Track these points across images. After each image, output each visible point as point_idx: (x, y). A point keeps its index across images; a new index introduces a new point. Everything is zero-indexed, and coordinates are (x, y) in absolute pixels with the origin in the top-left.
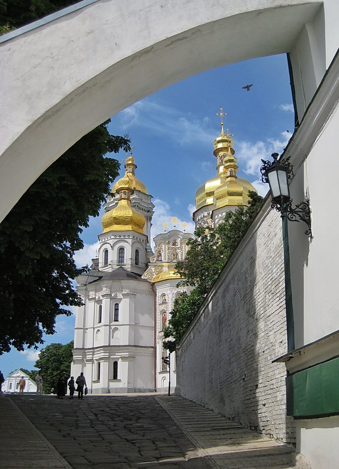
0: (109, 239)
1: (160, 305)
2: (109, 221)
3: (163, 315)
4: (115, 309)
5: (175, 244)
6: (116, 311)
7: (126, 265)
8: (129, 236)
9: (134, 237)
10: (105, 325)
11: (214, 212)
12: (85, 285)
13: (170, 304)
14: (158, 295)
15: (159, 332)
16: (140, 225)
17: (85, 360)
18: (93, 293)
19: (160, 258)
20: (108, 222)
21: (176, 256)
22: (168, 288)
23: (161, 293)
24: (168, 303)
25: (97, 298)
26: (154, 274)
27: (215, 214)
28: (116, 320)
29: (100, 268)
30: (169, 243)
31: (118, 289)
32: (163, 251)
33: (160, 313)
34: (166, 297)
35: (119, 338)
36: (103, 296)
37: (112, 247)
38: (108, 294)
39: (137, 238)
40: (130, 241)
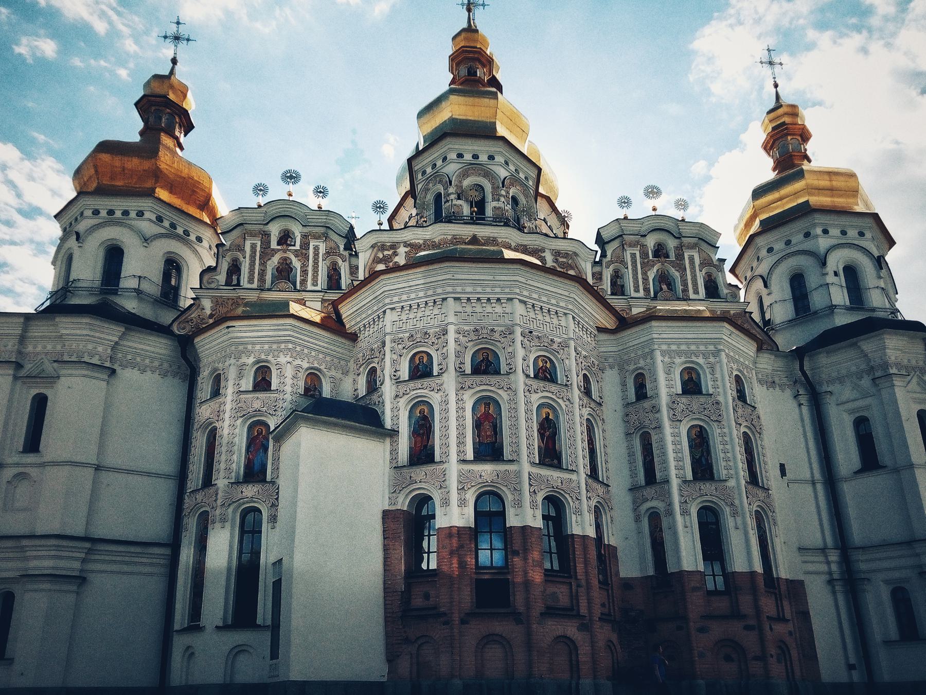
9: (160, 219)
19: (235, 277)
39: (173, 226)
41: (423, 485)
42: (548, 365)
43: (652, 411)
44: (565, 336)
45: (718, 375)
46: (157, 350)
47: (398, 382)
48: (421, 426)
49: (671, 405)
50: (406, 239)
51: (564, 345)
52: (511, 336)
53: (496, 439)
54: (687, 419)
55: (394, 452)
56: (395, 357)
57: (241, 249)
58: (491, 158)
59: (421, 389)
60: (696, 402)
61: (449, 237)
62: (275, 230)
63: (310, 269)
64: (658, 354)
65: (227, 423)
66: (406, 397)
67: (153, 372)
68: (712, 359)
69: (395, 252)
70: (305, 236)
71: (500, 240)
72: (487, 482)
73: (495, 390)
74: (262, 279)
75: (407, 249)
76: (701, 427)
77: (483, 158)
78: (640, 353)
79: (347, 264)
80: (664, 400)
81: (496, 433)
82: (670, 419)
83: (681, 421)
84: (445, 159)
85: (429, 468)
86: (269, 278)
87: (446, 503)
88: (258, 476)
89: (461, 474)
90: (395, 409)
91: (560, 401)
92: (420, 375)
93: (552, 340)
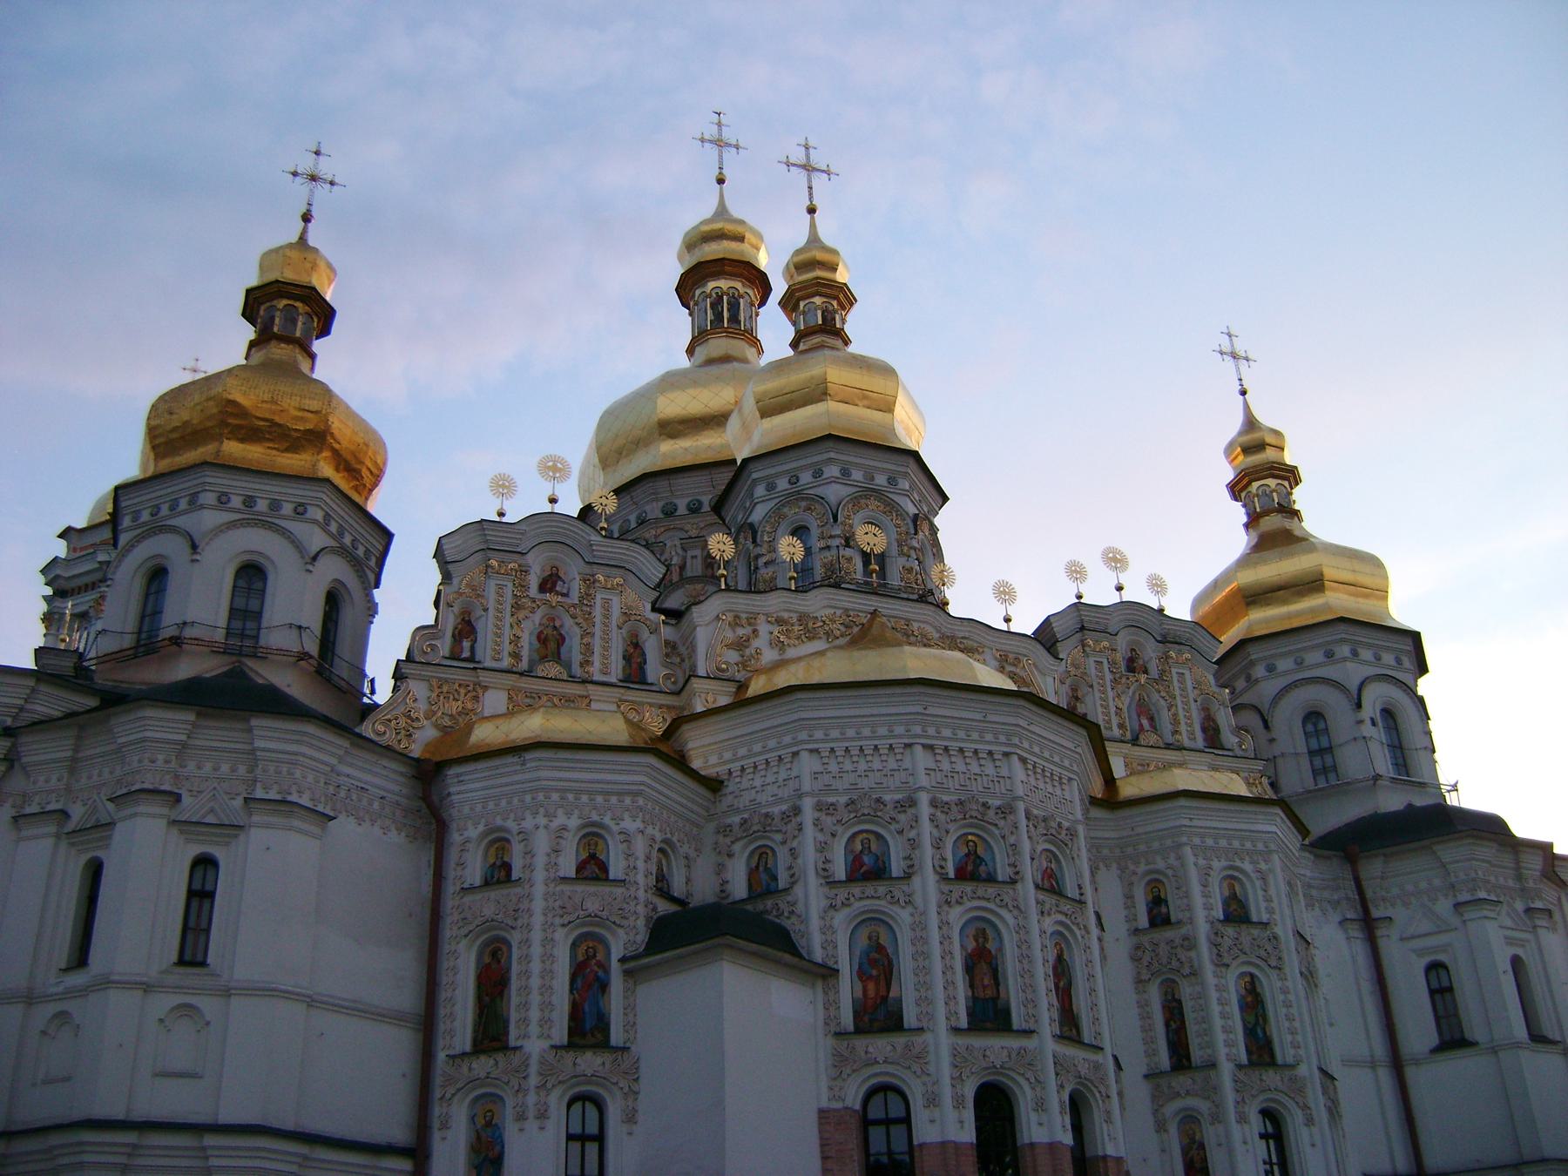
0: (183, 504)
3: (487, 959)
4: (191, 894)
5: (554, 585)
6: (195, 904)
8: (300, 509)
9: (327, 517)
11: (751, 466)
15: (452, 1057)
16: (355, 470)
19: (466, 644)
21: (552, 645)
23: (481, 828)
27: (754, 476)
28: (188, 957)
31: (225, 768)
39: (341, 532)
41: (890, 1069)
42: (1053, 866)
43: (1182, 946)
44: (1070, 817)
45: (1272, 892)
46: (392, 786)
47: (832, 883)
48: (873, 963)
49: (1213, 936)
50: (771, 609)
51: (1072, 833)
52: (1012, 817)
53: (998, 991)
54: (1240, 960)
55: (831, 1005)
56: (820, 837)
57: (477, 592)
58: (892, 481)
59: (868, 899)
60: (1247, 935)
61: (839, 612)
62: (537, 566)
64: (1187, 850)
65: (537, 935)
66: (846, 911)
67: (373, 822)
68: (1263, 866)
69: (755, 631)
70: (589, 581)
71: (916, 625)
72: (995, 1067)
73: (991, 906)
74: (516, 656)
75: (776, 630)
76: (1252, 976)
77: (881, 480)
78: (1156, 845)
80: (1202, 929)
81: (997, 984)
82: (1212, 961)
83: (1228, 966)
84: (818, 474)
85: (900, 1040)
86: (525, 653)
88: (593, 1035)
89: (955, 1053)
90: (827, 929)
91: (1074, 928)
92: (865, 872)
93: (1060, 825)
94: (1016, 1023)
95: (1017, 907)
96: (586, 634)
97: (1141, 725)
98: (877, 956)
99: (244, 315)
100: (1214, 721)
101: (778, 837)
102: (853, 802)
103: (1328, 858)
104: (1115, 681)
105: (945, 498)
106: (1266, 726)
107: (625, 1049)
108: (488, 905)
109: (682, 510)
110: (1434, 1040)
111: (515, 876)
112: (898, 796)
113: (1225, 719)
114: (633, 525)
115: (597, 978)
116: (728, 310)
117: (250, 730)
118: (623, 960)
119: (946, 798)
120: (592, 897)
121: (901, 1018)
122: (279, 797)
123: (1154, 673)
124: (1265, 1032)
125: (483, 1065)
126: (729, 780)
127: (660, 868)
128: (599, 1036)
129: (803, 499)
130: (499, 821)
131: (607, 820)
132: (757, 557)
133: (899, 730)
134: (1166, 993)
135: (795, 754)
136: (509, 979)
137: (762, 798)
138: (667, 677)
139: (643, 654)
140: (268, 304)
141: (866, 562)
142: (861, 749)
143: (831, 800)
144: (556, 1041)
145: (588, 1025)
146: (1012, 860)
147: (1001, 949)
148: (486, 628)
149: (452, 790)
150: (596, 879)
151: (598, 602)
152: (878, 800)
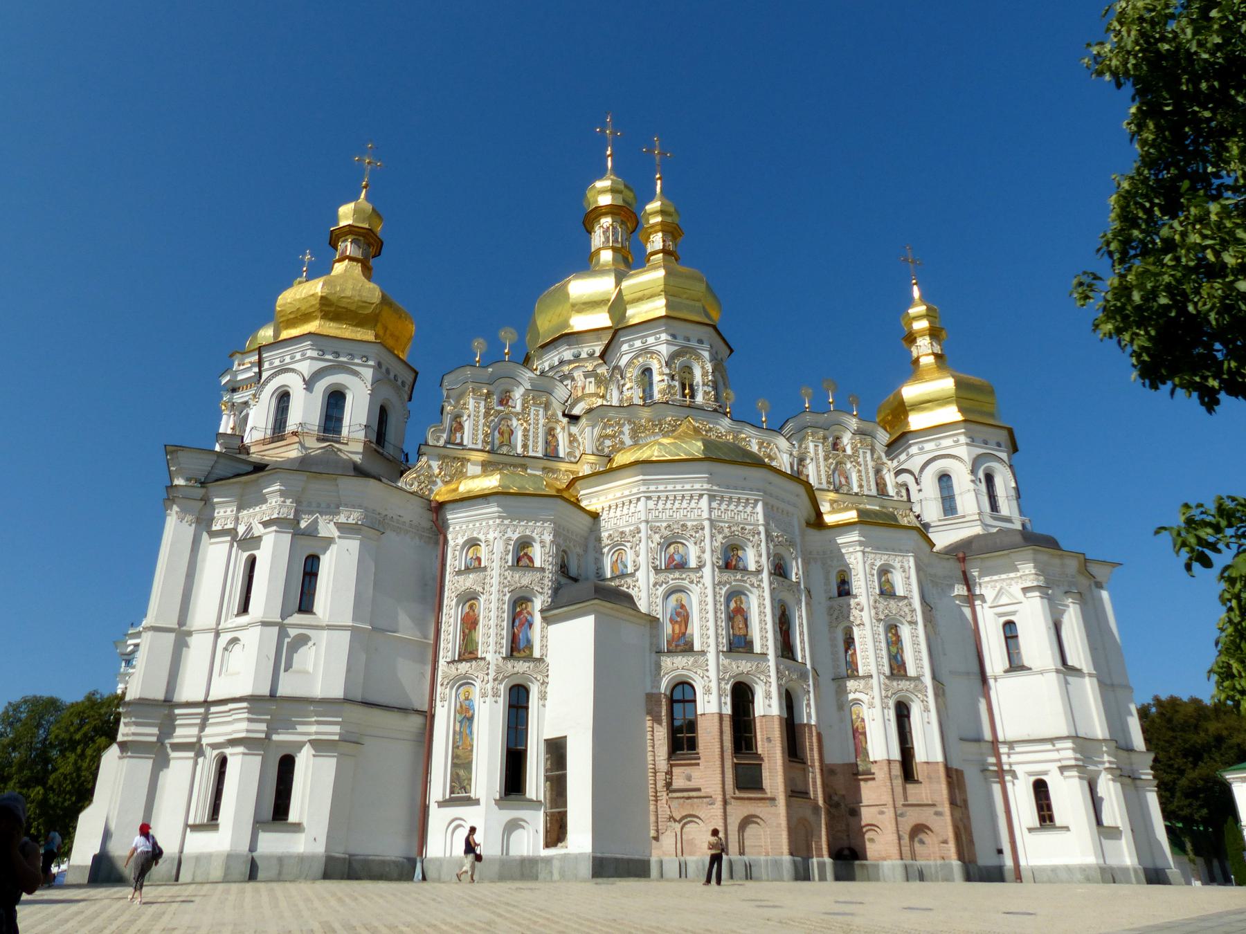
0: (298, 356)
1: (459, 573)
2: (303, 308)
4: (305, 574)
7: (347, 444)
8: (364, 359)
9: (379, 365)
10: (265, 624)
12: (203, 484)
13: (495, 573)
14: (451, 543)
15: (448, 663)
17: (168, 746)
18: (229, 513)
19: (458, 435)
20: (299, 309)
21: (506, 436)
22: (491, 522)
23: (465, 538)
24: (489, 569)
25: (241, 530)
26: (438, 480)
28: (303, 608)
29: (257, 443)
30: (489, 395)
32: (469, 416)
33: (455, 600)
34: (483, 552)
35: (311, 670)
36: (266, 524)
37: (309, 384)
38: (285, 519)
39: (388, 371)
40: (368, 373)
47: (657, 570)
48: (678, 614)
56: (653, 546)
63: (531, 433)
73: (747, 585)
79: (566, 434)
81: (747, 626)
87: (708, 691)
94: (757, 648)
95: (759, 586)
96: (526, 430)
97: (840, 481)
98: (681, 610)
99: (330, 244)
100: (884, 479)
101: (628, 545)
102: (669, 526)
103: (948, 559)
104: (826, 458)
105: (732, 351)
106: (918, 483)
107: (541, 660)
108: (469, 581)
109: (584, 355)
110: (1007, 666)
111: (483, 565)
112: (695, 523)
113: (889, 479)
114: (557, 363)
115: (527, 620)
116: (613, 235)
117: (337, 485)
118: (542, 611)
119: (722, 524)
120: (526, 579)
121: (692, 644)
122: (354, 522)
123: (849, 451)
124: (902, 657)
125: (464, 667)
126: (602, 512)
127: (563, 561)
128: (527, 652)
129: (649, 353)
130: (475, 535)
131: (534, 535)
132: (623, 385)
133: (697, 486)
134: (846, 634)
135: (639, 499)
136: (479, 621)
137: (621, 523)
138: (569, 454)
139: (557, 441)
140: (343, 238)
141: (684, 388)
142: (675, 497)
143: (658, 524)
144: (504, 656)
145: (522, 647)
146: (757, 559)
147: (749, 608)
148: (467, 426)
149: (448, 517)
150: (528, 566)
151: (532, 410)
152: (683, 525)
